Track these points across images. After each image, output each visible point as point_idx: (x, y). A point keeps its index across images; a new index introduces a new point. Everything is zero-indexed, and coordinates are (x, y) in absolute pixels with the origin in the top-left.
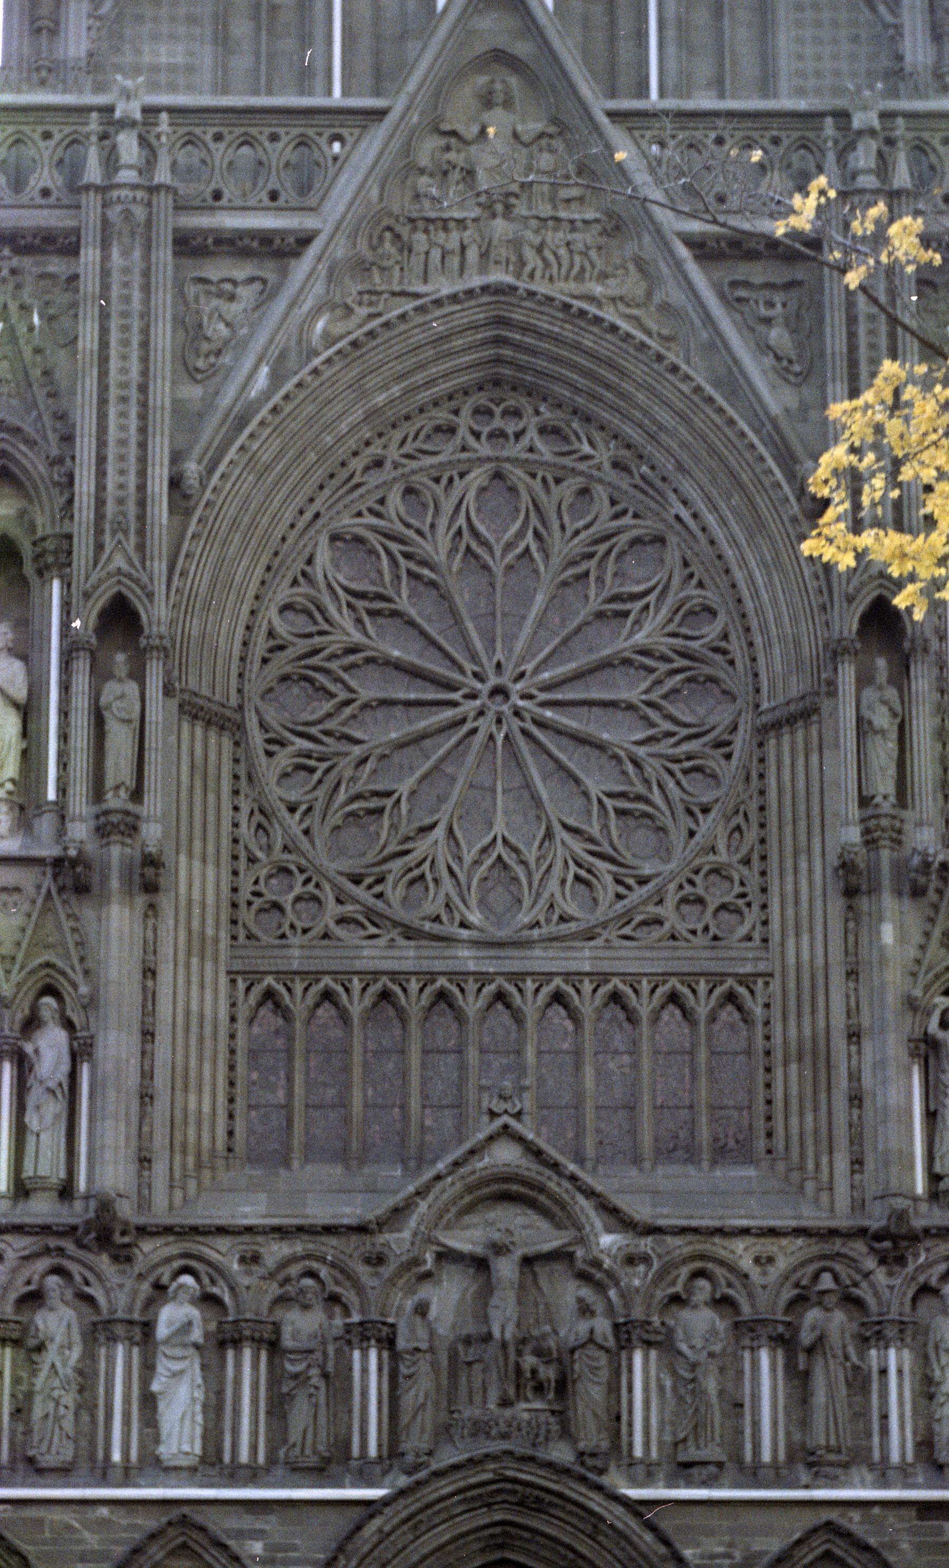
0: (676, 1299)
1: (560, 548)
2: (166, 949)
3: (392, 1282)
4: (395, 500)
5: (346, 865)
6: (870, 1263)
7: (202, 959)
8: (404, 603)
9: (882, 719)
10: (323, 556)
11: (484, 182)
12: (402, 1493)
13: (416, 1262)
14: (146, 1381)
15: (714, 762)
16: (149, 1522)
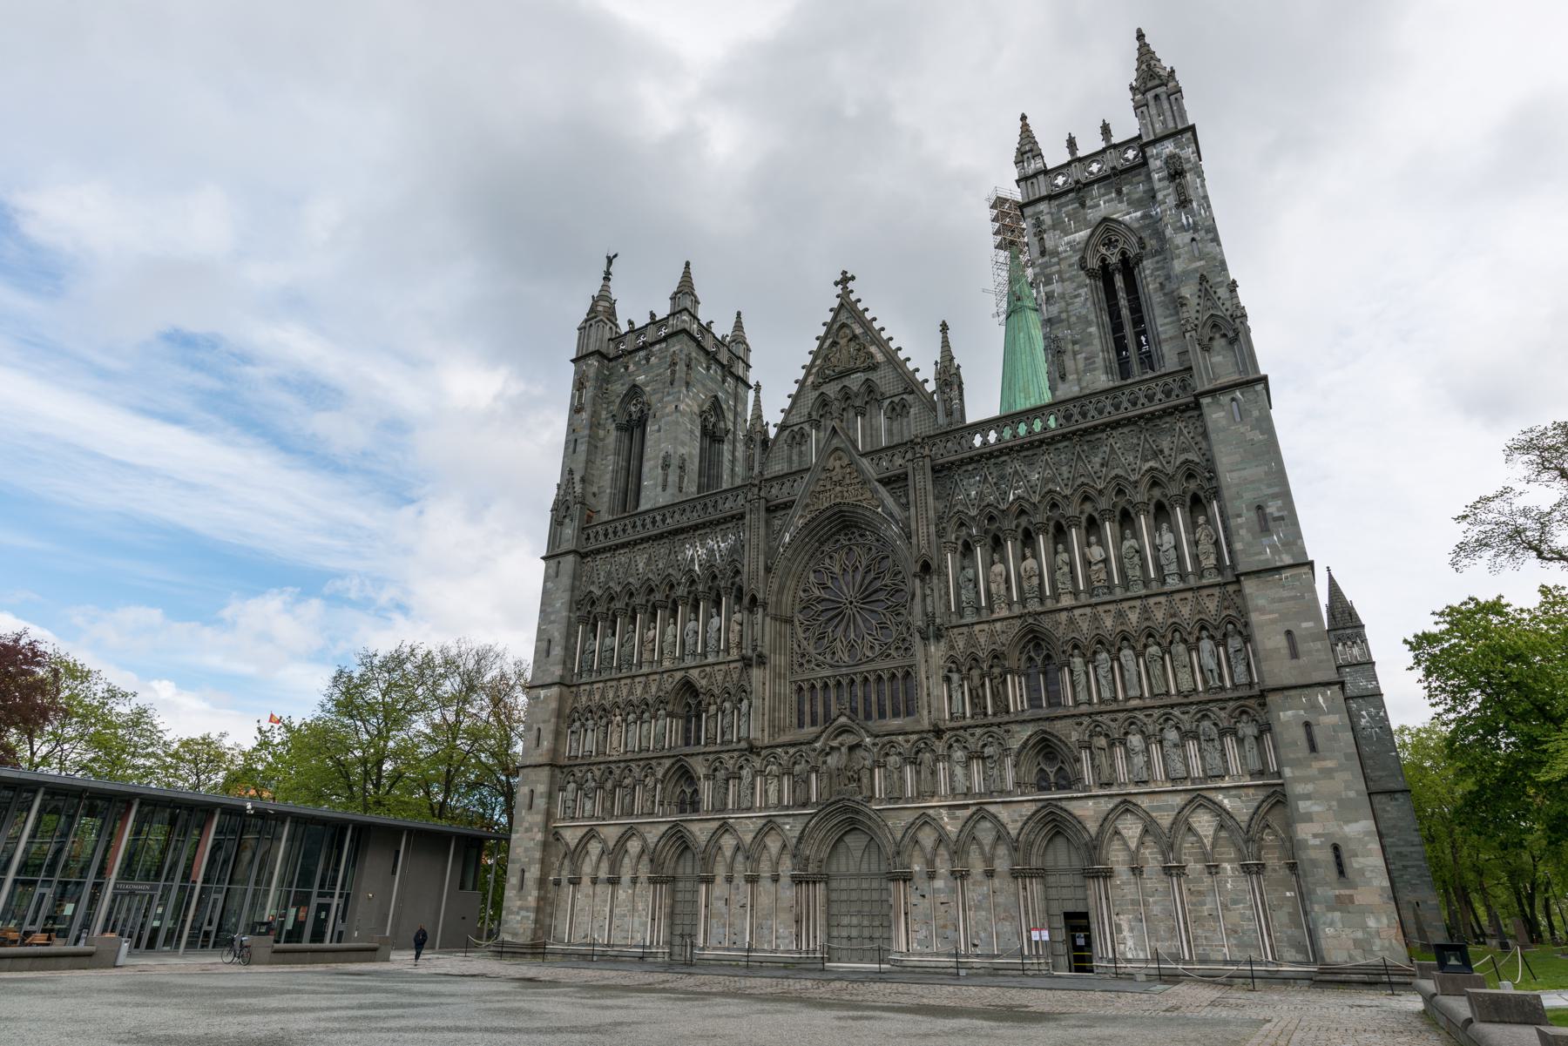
0: (887, 754)
1: (864, 563)
2: (768, 677)
3: (818, 755)
4: (827, 561)
5: (818, 651)
6: (934, 739)
7: (780, 678)
8: (830, 584)
9: (928, 592)
10: (812, 576)
11: (834, 479)
12: (820, 811)
13: (823, 750)
14: (766, 784)
15: (903, 611)
16: (764, 821)
